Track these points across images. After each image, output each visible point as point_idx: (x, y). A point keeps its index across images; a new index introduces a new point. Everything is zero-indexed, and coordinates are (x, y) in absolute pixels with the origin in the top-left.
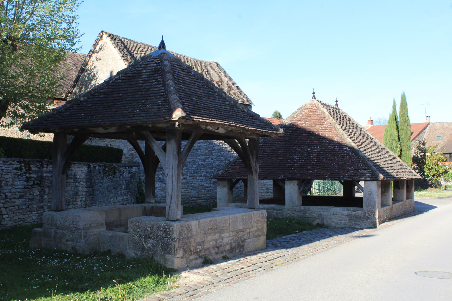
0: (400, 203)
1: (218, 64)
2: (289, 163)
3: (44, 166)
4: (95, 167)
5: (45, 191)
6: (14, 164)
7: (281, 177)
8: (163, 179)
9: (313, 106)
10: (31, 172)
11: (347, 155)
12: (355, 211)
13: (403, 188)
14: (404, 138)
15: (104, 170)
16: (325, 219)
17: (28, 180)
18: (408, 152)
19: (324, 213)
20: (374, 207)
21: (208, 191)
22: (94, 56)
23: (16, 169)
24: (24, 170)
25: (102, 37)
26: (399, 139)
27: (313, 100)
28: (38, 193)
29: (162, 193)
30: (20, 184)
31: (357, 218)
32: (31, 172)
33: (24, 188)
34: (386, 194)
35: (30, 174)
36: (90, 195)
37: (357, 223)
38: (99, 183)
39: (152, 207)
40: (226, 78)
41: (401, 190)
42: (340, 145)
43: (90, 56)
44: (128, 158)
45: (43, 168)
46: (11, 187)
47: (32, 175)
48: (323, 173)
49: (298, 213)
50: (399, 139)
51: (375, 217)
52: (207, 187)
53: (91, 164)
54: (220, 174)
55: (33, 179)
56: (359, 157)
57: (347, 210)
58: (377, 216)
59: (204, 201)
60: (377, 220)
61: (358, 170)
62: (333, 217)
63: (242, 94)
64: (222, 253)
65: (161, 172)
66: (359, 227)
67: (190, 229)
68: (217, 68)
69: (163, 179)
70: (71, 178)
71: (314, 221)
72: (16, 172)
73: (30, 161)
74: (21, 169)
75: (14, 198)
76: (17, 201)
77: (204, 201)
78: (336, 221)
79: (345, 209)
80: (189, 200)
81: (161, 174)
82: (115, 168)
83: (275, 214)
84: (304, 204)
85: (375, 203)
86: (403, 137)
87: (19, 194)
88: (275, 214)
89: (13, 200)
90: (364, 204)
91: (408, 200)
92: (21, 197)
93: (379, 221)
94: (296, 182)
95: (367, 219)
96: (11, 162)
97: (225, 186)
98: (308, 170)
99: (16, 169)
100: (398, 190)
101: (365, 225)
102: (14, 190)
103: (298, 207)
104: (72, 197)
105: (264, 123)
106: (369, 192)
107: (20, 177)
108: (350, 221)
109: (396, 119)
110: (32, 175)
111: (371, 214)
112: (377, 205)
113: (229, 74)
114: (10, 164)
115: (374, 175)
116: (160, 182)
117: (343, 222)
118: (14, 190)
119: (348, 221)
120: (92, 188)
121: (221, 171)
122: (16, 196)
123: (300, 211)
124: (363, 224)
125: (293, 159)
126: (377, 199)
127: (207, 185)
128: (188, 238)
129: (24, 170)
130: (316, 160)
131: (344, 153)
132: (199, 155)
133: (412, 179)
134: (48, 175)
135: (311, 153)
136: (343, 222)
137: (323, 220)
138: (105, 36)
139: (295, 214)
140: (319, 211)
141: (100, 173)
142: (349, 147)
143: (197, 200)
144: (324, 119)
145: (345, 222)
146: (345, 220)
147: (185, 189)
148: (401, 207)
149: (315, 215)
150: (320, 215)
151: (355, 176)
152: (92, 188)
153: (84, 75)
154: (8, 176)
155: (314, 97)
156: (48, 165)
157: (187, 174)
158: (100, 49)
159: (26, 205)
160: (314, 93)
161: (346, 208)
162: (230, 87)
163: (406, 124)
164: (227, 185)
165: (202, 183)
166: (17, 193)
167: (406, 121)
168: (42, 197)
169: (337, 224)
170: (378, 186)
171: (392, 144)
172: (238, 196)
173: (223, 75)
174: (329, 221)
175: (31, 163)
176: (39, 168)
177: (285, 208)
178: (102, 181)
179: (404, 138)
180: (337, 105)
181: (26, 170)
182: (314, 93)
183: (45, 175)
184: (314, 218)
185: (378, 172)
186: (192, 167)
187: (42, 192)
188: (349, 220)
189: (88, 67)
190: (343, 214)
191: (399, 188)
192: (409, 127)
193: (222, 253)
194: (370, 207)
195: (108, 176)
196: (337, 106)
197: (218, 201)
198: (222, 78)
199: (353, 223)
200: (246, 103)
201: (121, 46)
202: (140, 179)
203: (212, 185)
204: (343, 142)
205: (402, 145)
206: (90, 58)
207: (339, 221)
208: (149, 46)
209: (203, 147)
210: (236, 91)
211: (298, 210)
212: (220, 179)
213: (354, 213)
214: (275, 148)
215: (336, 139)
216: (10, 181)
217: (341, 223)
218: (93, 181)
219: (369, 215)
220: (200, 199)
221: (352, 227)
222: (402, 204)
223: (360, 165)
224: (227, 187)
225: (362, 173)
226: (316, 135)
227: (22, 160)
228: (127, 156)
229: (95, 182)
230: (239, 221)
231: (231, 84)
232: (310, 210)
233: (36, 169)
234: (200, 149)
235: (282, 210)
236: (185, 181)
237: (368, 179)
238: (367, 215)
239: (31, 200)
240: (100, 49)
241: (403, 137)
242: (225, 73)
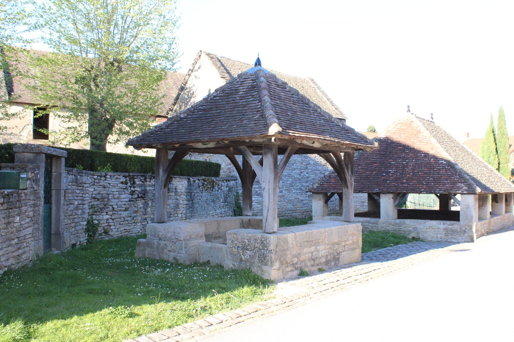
0: (499, 217)
2: (384, 176)
3: (147, 180)
4: (194, 181)
5: (148, 204)
6: (120, 179)
7: (376, 190)
9: (407, 120)
10: (135, 185)
13: (501, 202)
14: (502, 151)
15: (203, 184)
16: (421, 232)
17: (132, 193)
18: (506, 165)
20: (471, 221)
21: (304, 204)
22: (193, 74)
23: (122, 183)
24: (129, 184)
25: (200, 56)
26: (497, 151)
27: (409, 113)
28: (142, 206)
29: (259, 206)
30: (125, 197)
31: (453, 231)
32: (135, 185)
33: (129, 201)
34: (484, 208)
35: (134, 187)
36: (190, 207)
38: (198, 196)
39: (249, 220)
40: (320, 93)
41: (499, 204)
42: (436, 159)
43: (189, 75)
44: (226, 172)
45: (146, 181)
46: (117, 200)
47: (136, 189)
50: (497, 151)
52: (302, 200)
53: (191, 178)
54: (315, 187)
55: (137, 192)
57: (443, 224)
58: (474, 230)
61: (454, 183)
62: (428, 230)
63: (336, 109)
64: (318, 265)
65: (258, 186)
66: (456, 241)
67: (286, 241)
68: (311, 83)
70: (172, 192)
72: (121, 185)
73: (134, 176)
74: (126, 183)
75: (120, 210)
76: (122, 213)
78: (432, 234)
79: (442, 223)
80: (285, 213)
81: (258, 188)
82: (213, 182)
84: (399, 218)
85: (472, 217)
86: (501, 149)
87: (125, 206)
89: (120, 212)
90: (460, 218)
91: (507, 214)
92: (126, 210)
94: (391, 196)
95: (464, 233)
96: (117, 176)
99: (122, 183)
100: (497, 204)
101: (462, 239)
102: (120, 203)
103: (393, 221)
104: (173, 210)
105: (359, 137)
107: (125, 190)
108: (446, 235)
109: (493, 132)
110: (136, 189)
112: (474, 219)
113: (323, 89)
114: (117, 178)
115: (472, 188)
116: (257, 195)
117: (439, 235)
118: (120, 203)
119: (444, 235)
120: (192, 201)
121: (317, 185)
122: (122, 209)
124: (460, 238)
125: (387, 173)
126: (475, 212)
127: (303, 198)
128: (284, 250)
129: (129, 184)
130: (411, 174)
132: (294, 169)
133: (511, 193)
134: (151, 188)
135: (406, 166)
136: (439, 235)
137: (418, 233)
138: (203, 55)
139: (390, 228)
141: (199, 187)
142: (445, 160)
143: (293, 213)
144: (419, 132)
145: (441, 235)
147: (281, 203)
148: (499, 221)
149: (411, 229)
151: (451, 189)
152: (192, 201)
153: (184, 93)
154: (114, 190)
156: (150, 179)
157: (282, 188)
158: (199, 68)
159: (131, 217)
160: (409, 107)
161: (442, 222)
162: (324, 102)
163: (504, 137)
164: (322, 198)
166: (123, 206)
167: (504, 134)
168: (145, 210)
169: (433, 237)
170: (475, 200)
171: (490, 157)
173: (317, 90)
175: (135, 177)
176: (143, 182)
178: (201, 194)
179: (502, 151)
181: (131, 184)
182: (409, 107)
183: (148, 188)
184: (410, 232)
185: (475, 185)
186: (287, 181)
187: (146, 204)
188: (445, 234)
189: (188, 86)
190: (439, 228)
191: (497, 202)
192: (507, 140)
193: (318, 265)
195: (207, 190)
197: (313, 214)
199: (450, 237)
200: (341, 118)
201: (219, 64)
202: (237, 193)
203: (307, 198)
204: (439, 155)
205: (500, 158)
206: (189, 76)
207: (435, 235)
208: (245, 63)
209: (299, 162)
210: (331, 105)
212: (315, 192)
213: (450, 227)
215: (432, 152)
216: (117, 195)
217: (437, 237)
218: (193, 194)
219: (466, 229)
221: (449, 240)
222: (500, 218)
223: (456, 178)
225: (458, 187)
226: (411, 148)
227: (127, 174)
228: (225, 170)
229: (194, 195)
230: (334, 234)
231: (326, 99)
232: (404, 223)
233: (140, 183)
234: (295, 163)
235: (377, 224)
236: (281, 194)
237: (465, 192)
238: (464, 228)
239: (136, 212)
240: (199, 68)
241: (501, 149)
242: (319, 88)
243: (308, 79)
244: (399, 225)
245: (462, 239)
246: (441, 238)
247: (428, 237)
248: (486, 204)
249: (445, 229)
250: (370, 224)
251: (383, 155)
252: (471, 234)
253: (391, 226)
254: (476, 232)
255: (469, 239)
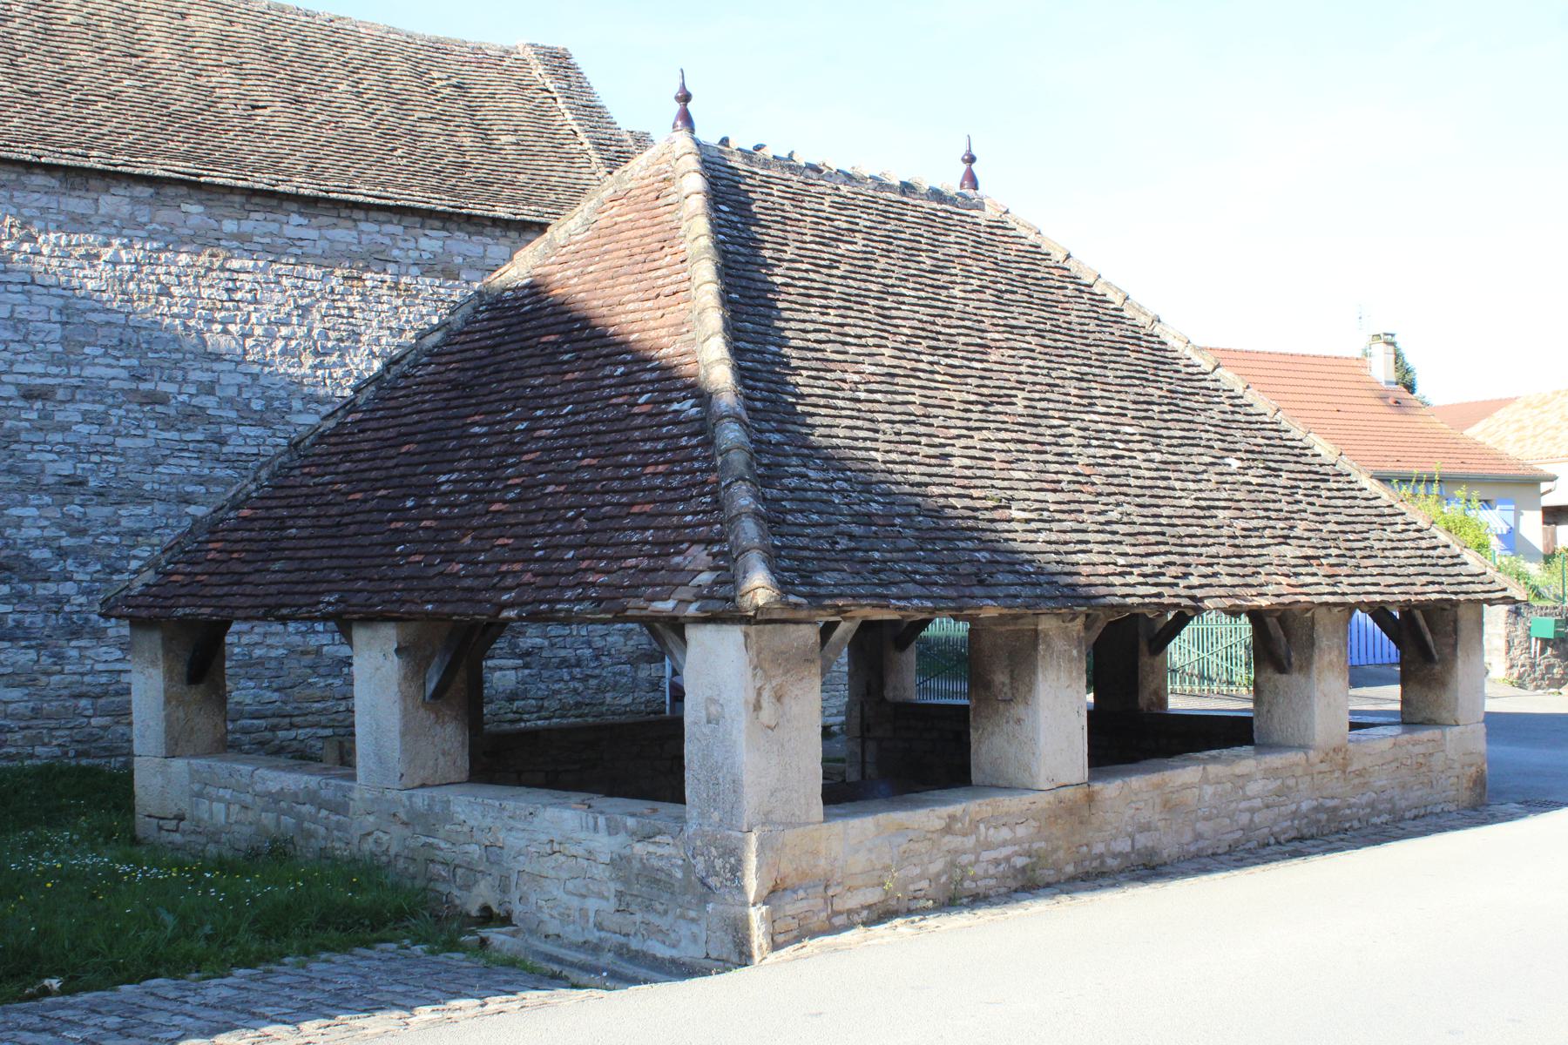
1: (559, 62)
8: (18, 624)
11: (664, 451)
12: (647, 838)
16: (514, 877)
19: (514, 841)
29: (15, 694)
31: (655, 879)
34: (1018, 710)
37: (653, 918)
41: (1295, 678)
48: (504, 574)
49: (407, 832)
51: (741, 889)
54: (137, 587)
56: (713, 457)
57: (612, 830)
59: (329, 732)
60: (757, 917)
61: (666, 547)
68: (538, 70)
69: (18, 624)
71: (467, 887)
77: (329, 732)
78: (558, 893)
79: (601, 820)
83: (322, 831)
88: (322, 831)
93: (772, 920)
95: (703, 901)
97: (153, 663)
98: (449, 557)
100: (1284, 677)
101: (694, 939)
103: (404, 795)
106: (711, 700)
111: (719, 863)
117: (592, 904)
119: (612, 904)
123: (414, 820)
124: (684, 930)
131: (659, 439)
135: (515, 450)
139: (393, 840)
140: (488, 822)
143: (274, 728)
146: (601, 896)
148: (1254, 788)
149: (475, 850)
150: (492, 851)
155: (686, 119)
160: (685, 98)
164: (160, 654)
165: (313, 641)
169: (565, 918)
172: (578, 705)
174: (533, 899)
177: (356, 795)
180: (971, 180)
182: (685, 98)
190: (590, 856)
191: (1282, 667)
194: (716, 816)
196: (976, 187)
198: (541, 116)
199: (638, 917)
207: (575, 902)
211: (403, 815)
213: (640, 849)
214: (392, 432)
217: (583, 912)
219: (711, 870)
220: (292, 726)
221: (635, 944)
222: (1272, 773)
224: (161, 663)
225: (678, 570)
230: (121, 868)
231: (587, 145)
232: (448, 818)
235: (341, 808)
237: (692, 610)
243: (528, 54)
244: (423, 821)
245: (695, 938)
246: (600, 927)
247: (546, 917)
248: (1031, 687)
249: (618, 863)
250: (324, 813)
251: (464, 386)
252: (738, 909)
253: (397, 830)
254: (774, 894)
255: (722, 945)
